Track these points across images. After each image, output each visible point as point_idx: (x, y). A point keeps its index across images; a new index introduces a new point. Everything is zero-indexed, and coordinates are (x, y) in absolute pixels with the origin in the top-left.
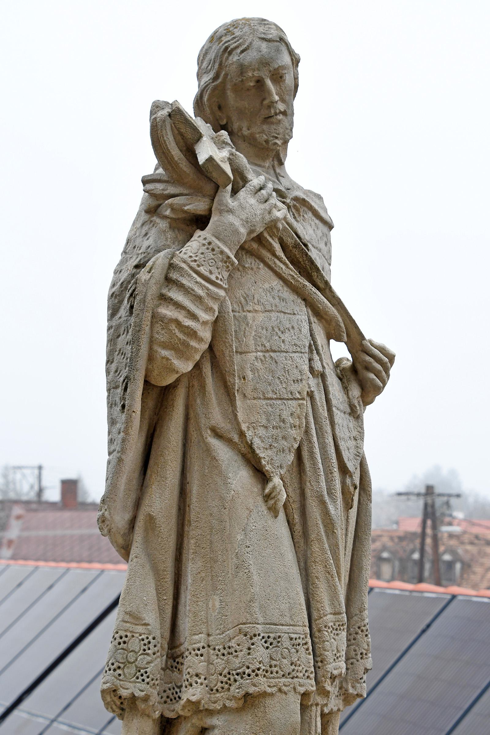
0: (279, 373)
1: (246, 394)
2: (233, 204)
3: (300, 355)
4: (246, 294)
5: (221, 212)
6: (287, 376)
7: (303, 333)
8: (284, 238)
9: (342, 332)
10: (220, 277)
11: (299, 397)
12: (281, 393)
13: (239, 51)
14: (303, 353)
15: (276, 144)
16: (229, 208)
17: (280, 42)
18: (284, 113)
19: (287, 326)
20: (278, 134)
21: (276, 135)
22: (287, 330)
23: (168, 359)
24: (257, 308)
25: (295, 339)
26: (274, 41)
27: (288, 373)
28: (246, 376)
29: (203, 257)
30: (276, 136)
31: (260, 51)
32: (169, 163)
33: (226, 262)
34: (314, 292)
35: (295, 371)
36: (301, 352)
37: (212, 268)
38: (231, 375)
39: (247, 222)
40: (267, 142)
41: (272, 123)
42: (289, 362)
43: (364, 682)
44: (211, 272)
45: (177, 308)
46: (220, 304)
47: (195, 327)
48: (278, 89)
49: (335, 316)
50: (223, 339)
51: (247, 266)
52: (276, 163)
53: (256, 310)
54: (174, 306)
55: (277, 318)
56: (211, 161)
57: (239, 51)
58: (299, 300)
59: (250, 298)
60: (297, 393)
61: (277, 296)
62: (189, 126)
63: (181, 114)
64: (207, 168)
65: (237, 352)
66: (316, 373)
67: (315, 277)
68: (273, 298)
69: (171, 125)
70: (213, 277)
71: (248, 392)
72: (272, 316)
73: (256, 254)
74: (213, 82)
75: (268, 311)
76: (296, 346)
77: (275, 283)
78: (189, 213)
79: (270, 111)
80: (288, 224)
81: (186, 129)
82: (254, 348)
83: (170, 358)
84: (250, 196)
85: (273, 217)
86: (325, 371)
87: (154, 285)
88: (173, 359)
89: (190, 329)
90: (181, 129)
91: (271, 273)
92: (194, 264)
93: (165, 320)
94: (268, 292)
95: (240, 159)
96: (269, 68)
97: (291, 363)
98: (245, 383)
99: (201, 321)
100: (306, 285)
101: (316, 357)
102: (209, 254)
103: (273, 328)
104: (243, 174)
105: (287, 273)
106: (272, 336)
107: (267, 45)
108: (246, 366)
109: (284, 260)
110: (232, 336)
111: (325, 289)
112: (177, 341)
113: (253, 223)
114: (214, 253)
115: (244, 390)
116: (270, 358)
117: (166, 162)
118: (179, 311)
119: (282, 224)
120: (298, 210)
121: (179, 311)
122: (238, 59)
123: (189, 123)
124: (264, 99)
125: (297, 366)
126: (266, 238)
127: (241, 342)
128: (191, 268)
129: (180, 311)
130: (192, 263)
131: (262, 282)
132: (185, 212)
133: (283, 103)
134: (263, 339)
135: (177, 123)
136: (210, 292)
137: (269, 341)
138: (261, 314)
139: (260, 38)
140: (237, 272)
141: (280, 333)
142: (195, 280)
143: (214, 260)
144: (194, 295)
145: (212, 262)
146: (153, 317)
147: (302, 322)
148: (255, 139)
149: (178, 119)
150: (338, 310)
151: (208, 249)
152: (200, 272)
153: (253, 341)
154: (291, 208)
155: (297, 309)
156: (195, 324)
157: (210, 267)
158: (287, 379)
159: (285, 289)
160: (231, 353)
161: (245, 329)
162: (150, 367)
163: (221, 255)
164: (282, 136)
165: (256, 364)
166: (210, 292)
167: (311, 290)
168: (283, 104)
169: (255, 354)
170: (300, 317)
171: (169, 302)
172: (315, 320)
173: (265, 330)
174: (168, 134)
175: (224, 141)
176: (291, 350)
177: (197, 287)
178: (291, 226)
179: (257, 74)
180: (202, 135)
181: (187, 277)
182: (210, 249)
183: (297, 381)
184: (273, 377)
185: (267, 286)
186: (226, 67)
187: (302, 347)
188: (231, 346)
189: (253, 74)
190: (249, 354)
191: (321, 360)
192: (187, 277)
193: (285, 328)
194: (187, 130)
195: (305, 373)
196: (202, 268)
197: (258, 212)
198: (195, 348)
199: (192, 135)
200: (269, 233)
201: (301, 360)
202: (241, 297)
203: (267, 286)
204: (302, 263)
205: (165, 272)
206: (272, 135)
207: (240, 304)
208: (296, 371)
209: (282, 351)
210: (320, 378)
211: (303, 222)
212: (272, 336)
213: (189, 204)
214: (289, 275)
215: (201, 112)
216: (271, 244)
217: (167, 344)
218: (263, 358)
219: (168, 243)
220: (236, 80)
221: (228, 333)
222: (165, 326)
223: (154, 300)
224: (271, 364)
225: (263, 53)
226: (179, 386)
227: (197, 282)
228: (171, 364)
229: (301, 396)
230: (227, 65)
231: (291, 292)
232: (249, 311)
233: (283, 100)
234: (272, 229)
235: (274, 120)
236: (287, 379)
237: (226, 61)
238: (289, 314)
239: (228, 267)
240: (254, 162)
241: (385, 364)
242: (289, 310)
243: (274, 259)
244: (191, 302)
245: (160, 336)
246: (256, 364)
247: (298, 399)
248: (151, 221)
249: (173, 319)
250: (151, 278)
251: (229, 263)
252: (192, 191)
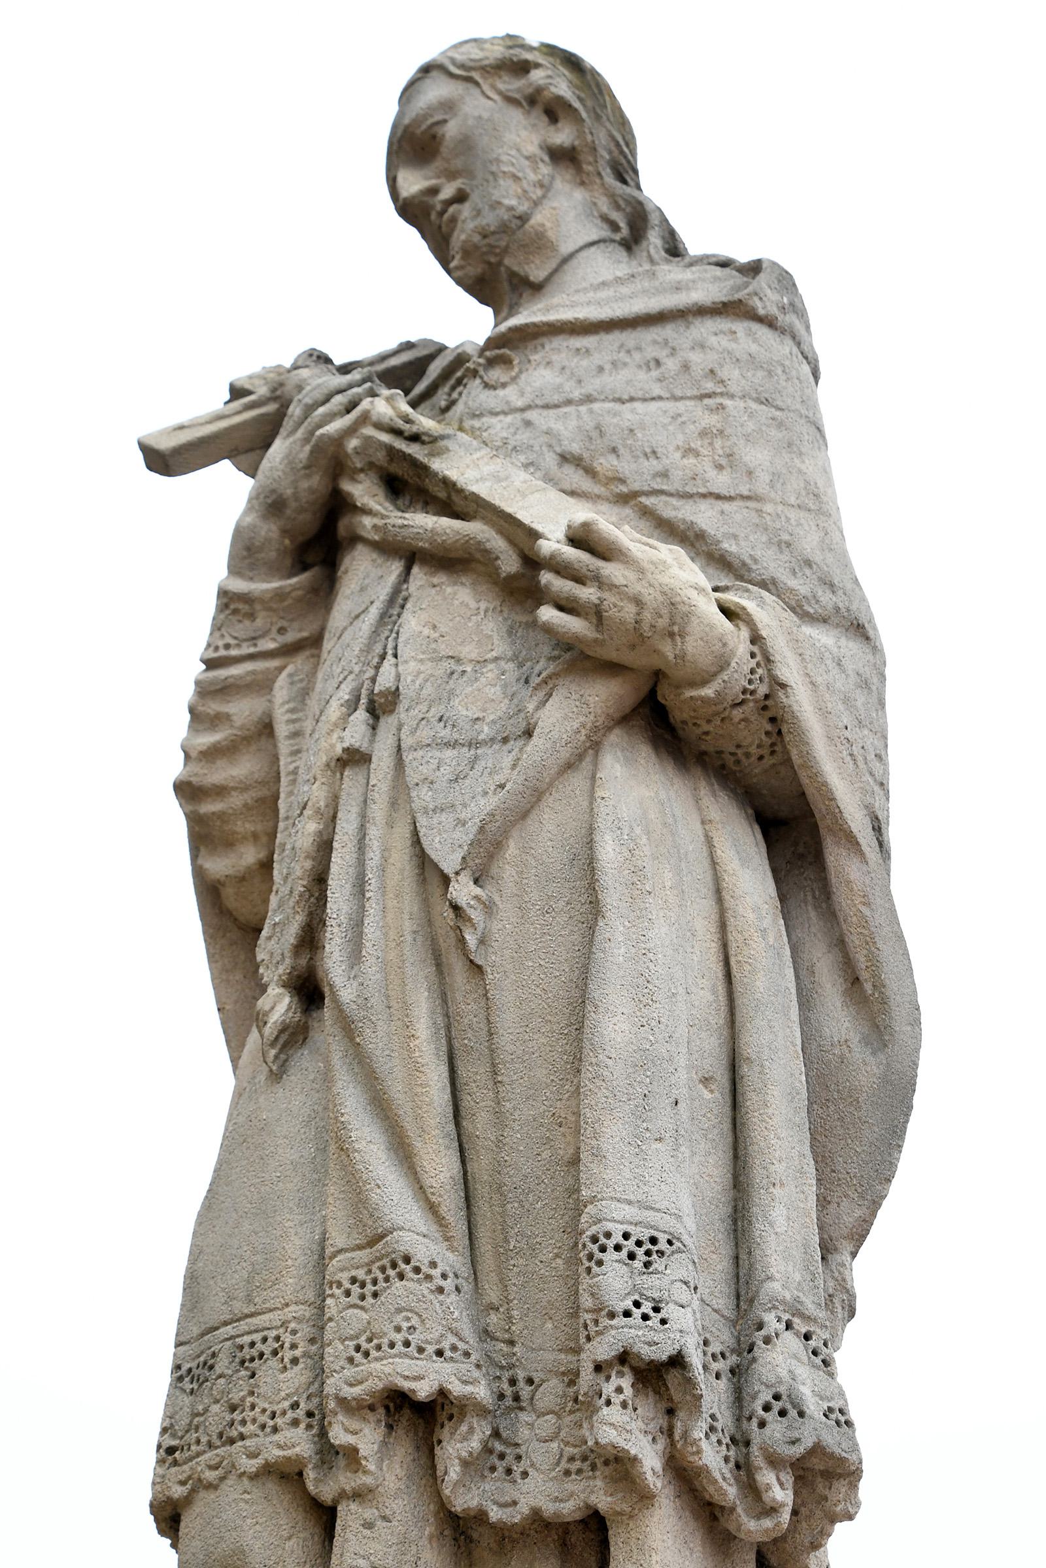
18: (461, 197)
43: (608, 1403)
67: (430, 488)
120: (506, 362)
150: (486, 520)
198: (213, 813)
233: (452, 175)
241: (552, 561)
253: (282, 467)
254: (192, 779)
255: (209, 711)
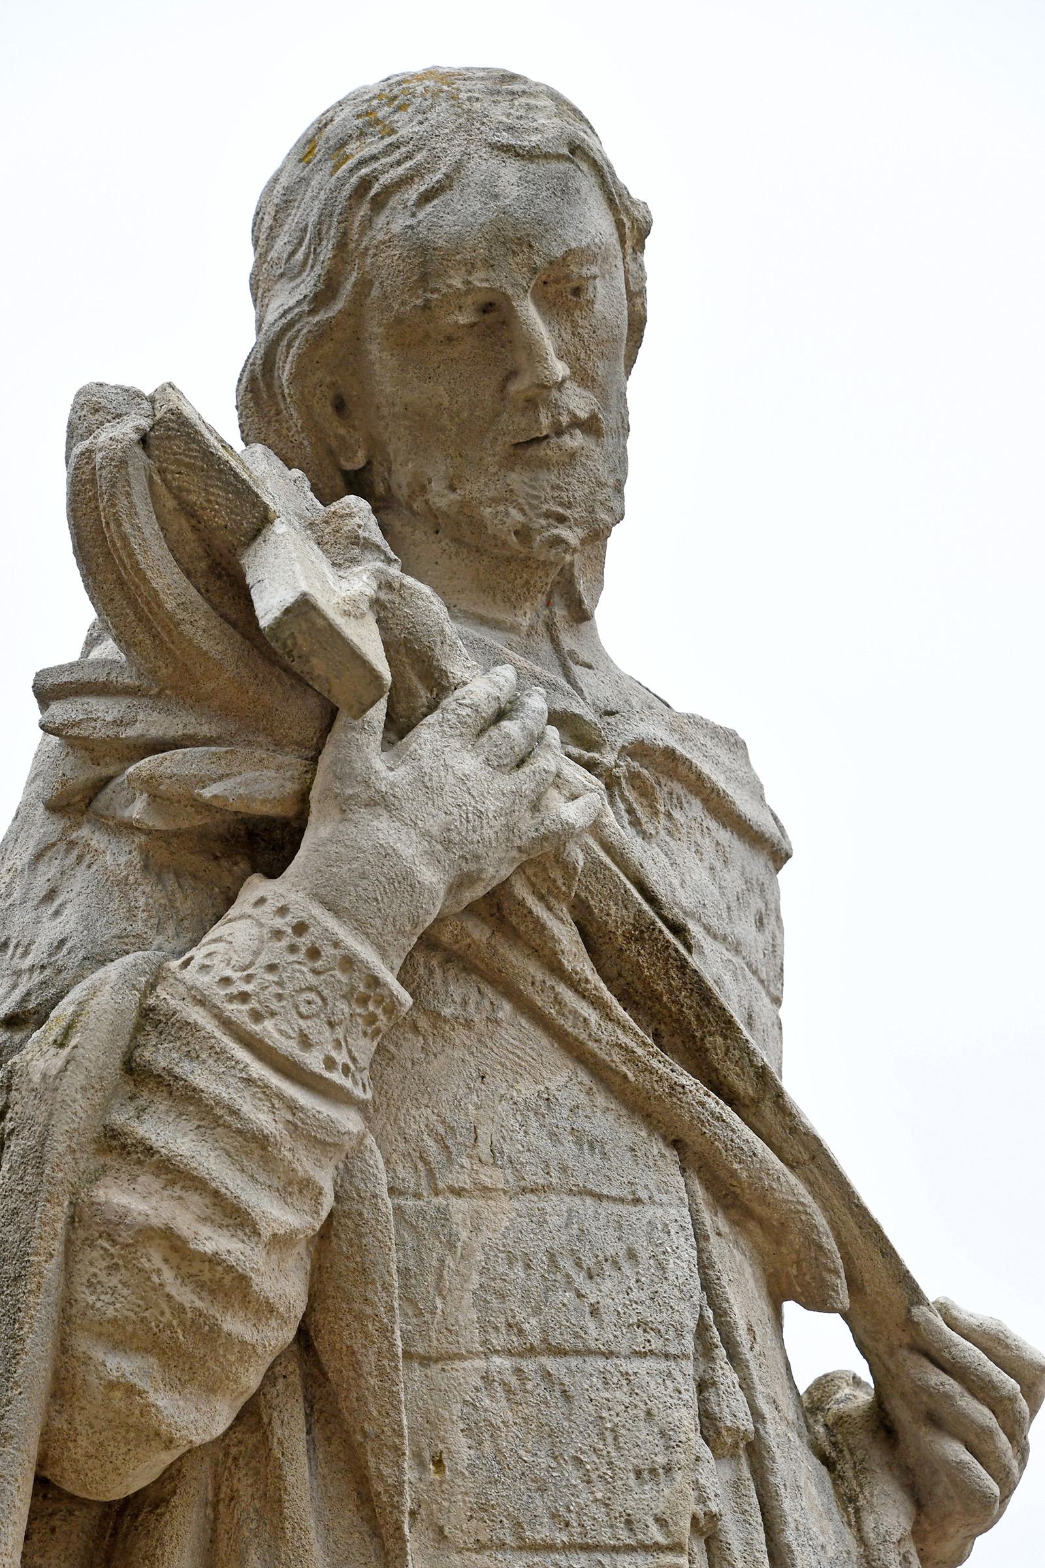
0: (579, 1442)
1: (446, 1530)
2: (391, 773)
3: (663, 1365)
4: (443, 1122)
5: (344, 807)
6: (613, 1454)
7: (672, 1278)
8: (592, 903)
9: (830, 1271)
10: (341, 1058)
11: (660, 1539)
12: (588, 1523)
13: (412, 194)
14: (676, 1357)
15: (558, 541)
16: (377, 792)
17: (573, 162)
18: (591, 426)
19: (610, 1251)
20: (569, 506)
21: (560, 510)
22: (607, 1267)
23: (131, 1391)
24: (491, 1177)
25: (643, 1303)
26: (547, 156)
27: (615, 1439)
28: (444, 1456)
29: (277, 983)
30: (558, 513)
31: (496, 196)
32: (140, 620)
33: (363, 1001)
34: (712, 1114)
35: (643, 1432)
36: (667, 1356)
37: (310, 1023)
38: (386, 1451)
39: (447, 844)
40: (524, 534)
41: (545, 464)
42: (618, 1394)
44: (305, 1042)
45: (172, 1183)
46: (341, 1166)
47: (242, 1257)
48: (564, 334)
49: (801, 1208)
50: (356, 1306)
51: (447, 1012)
52: (560, 612)
53: (487, 1188)
54: (158, 1176)
55: (570, 1217)
56: (305, 613)
57: (412, 194)
58: (657, 1147)
59: (460, 1139)
60: (650, 1521)
61: (569, 1128)
62: (219, 479)
63: (189, 434)
64: (289, 642)
65: (408, 1355)
66: (729, 1441)
67: (716, 1056)
68: (553, 1136)
69: (151, 477)
70: (313, 1061)
71: (452, 1519)
72: (549, 1210)
73: (483, 967)
74: (312, 312)
75: (532, 1191)
76: (645, 1331)
77: (561, 1079)
78: (219, 810)
79: (537, 421)
80: (608, 848)
81: (208, 493)
82: (477, 1339)
83: (141, 1384)
84: (458, 745)
85: (547, 822)
86: (762, 1432)
87: (79, 1096)
88: (151, 1391)
89: (219, 1268)
90: (189, 491)
91: (545, 1042)
92: (238, 1012)
93: (124, 1234)
94: (531, 1114)
95: (420, 602)
96: (529, 258)
97: (627, 1400)
98: (441, 1482)
99: (266, 1233)
100: (683, 1087)
101: (727, 1376)
102: (300, 971)
103: (552, 1257)
104: (432, 658)
105: (605, 1037)
106: (548, 1289)
107: (523, 174)
108: (447, 1415)
109: (596, 989)
110: (389, 1294)
111: (756, 1102)
112: (168, 1315)
113: (471, 847)
114: (318, 964)
115: (440, 1511)
116: (543, 1378)
117: (132, 617)
118: (180, 1198)
119: (587, 850)
121: (180, 1198)
122: (411, 227)
123: (221, 471)
124: (512, 375)
125: (649, 1413)
126: (521, 903)
127: (428, 1317)
128: (228, 1025)
129: (184, 1195)
130: (231, 1007)
131: (510, 1076)
132: (206, 807)
133: (586, 387)
134: (513, 1304)
135: (173, 472)
136: (301, 1119)
137: (537, 1311)
138: (505, 1203)
139: (492, 146)
140: (410, 1036)
141: (579, 1279)
142: (241, 1071)
143: (319, 994)
144: (239, 1132)
145: (309, 1003)
146: (73, 1221)
147: (669, 1233)
148: (478, 526)
149: (175, 454)
150: (810, 1184)
151: (293, 949)
152: (261, 1041)
153: (474, 1310)
154: (620, 784)
155: (647, 1181)
156: (240, 1245)
157: (301, 1022)
158: (610, 1463)
159: (601, 1100)
160: (386, 1362)
161: (442, 1261)
162: (60, 1423)
163: (344, 971)
164: (584, 514)
165: (487, 1402)
166: (301, 1119)
167: (702, 1104)
168: (585, 393)
169: (480, 1363)
170: (660, 1212)
171: (140, 1162)
172: (720, 1225)
173: (519, 1268)
174: (136, 514)
175: (357, 537)
176: (624, 1347)
177: (248, 1099)
178: (622, 854)
179: (482, 280)
180: (271, 515)
181: (211, 1061)
182: (304, 949)
183: (653, 1471)
184: (555, 1458)
185: (526, 1090)
186: (364, 254)
187: (671, 1334)
188: (386, 1332)
189: (469, 283)
190: (458, 1364)
191: (747, 1386)
192: (211, 1061)
193: (601, 1258)
194: (213, 494)
195: (683, 1439)
196: (268, 1024)
197: (491, 806)
198: (243, 1343)
199: (232, 512)
200: (533, 885)
201: (666, 1388)
202: (425, 1137)
203: (526, 1090)
204: (665, 999)
205: (123, 1041)
206: (545, 507)
207: (420, 1165)
208: (645, 1432)
209: (590, 1352)
210: (744, 1461)
211: (668, 839)
212: (548, 1289)
213: (221, 778)
214: (613, 1046)
215: (269, 422)
216: (540, 927)
217: (130, 1328)
218: (514, 1381)
219: (139, 927)
220: (403, 303)
221: (373, 1282)
222: (122, 1257)
223: (78, 1155)
224: (546, 1403)
225: (507, 201)
226: (175, 1500)
227: (249, 1081)
228: (143, 1412)
229: (668, 1534)
230: (367, 249)
231: (624, 1112)
232: (459, 1192)
233: (583, 377)
234: (545, 869)
235: (549, 452)
236: (610, 1463)
237: (362, 233)
238: (614, 1200)
239: (372, 1019)
240: (474, 609)
242: (617, 1183)
243: (553, 983)
244: (224, 1158)
245: (102, 1297)
246: (487, 1402)
247: (658, 1548)
248: (72, 844)
249: (152, 1229)
250: (70, 1068)
251: (378, 1003)
252: (233, 728)
253: (496, 824)
254: (253, 1276)
255: (296, 1165)
